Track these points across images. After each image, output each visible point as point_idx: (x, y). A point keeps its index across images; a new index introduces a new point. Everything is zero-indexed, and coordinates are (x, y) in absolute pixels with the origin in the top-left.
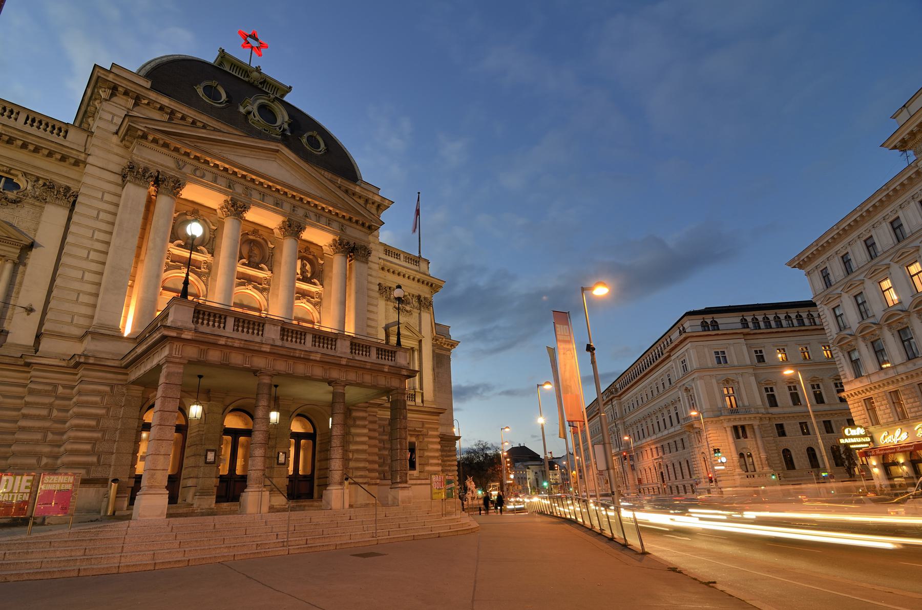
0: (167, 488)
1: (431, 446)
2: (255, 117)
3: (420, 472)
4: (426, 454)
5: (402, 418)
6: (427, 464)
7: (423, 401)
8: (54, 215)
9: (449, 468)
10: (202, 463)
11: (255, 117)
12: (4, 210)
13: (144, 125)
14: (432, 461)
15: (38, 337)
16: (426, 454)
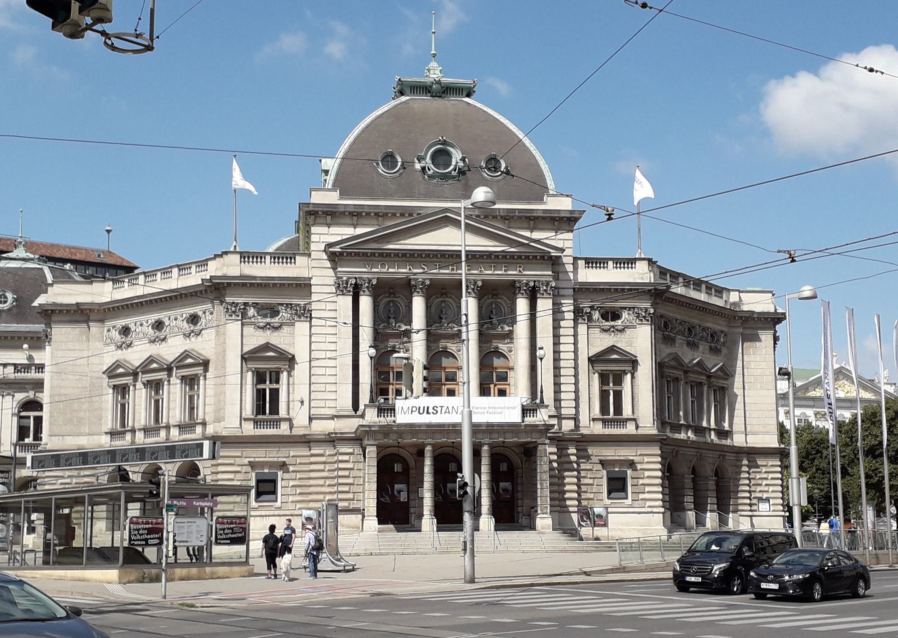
0: (377, 516)
1: (647, 474)
2: (429, 170)
3: (632, 500)
4: (641, 481)
5: (542, 463)
6: (644, 493)
7: (637, 427)
8: (302, 327)
9: (766, 489)
10: (417, 498)
11: (429, 170)
12: (275, 334)
13: (338, 247)
14: (647, 489)
15: (311, 419)
16: (641, 481)
